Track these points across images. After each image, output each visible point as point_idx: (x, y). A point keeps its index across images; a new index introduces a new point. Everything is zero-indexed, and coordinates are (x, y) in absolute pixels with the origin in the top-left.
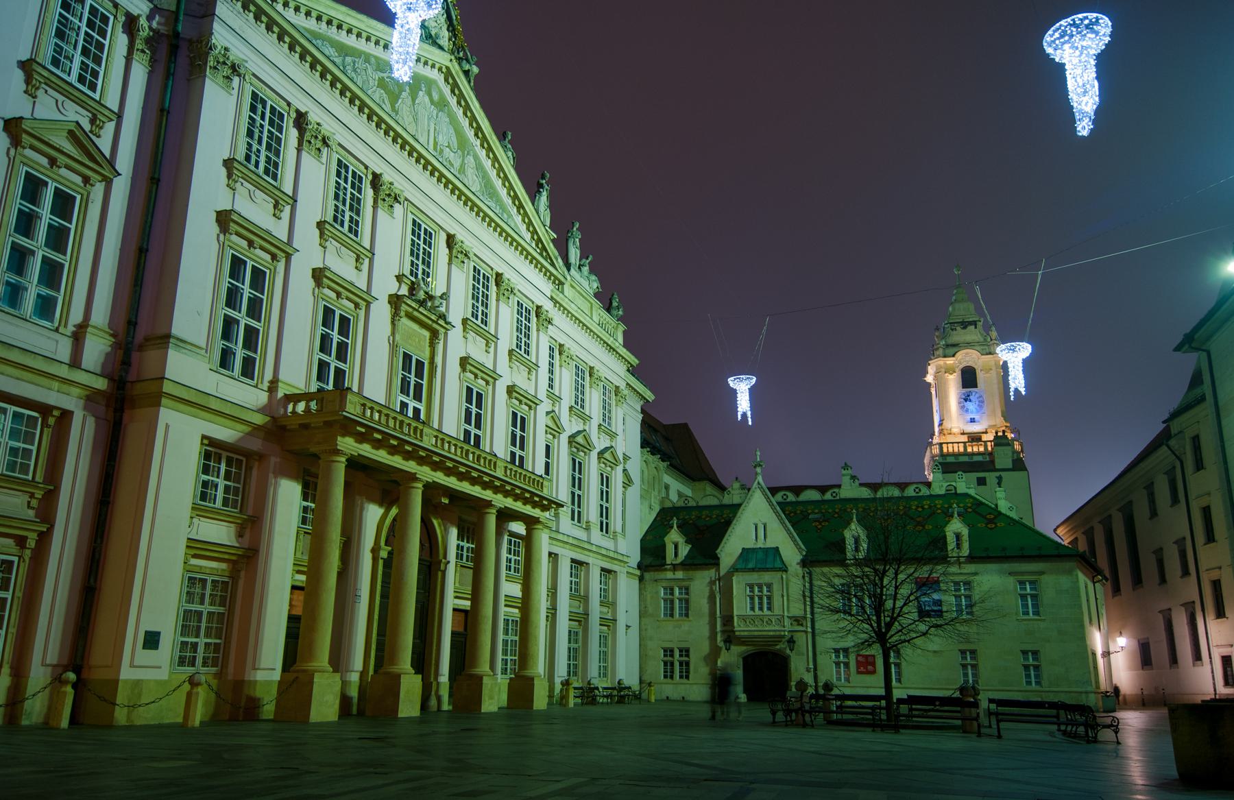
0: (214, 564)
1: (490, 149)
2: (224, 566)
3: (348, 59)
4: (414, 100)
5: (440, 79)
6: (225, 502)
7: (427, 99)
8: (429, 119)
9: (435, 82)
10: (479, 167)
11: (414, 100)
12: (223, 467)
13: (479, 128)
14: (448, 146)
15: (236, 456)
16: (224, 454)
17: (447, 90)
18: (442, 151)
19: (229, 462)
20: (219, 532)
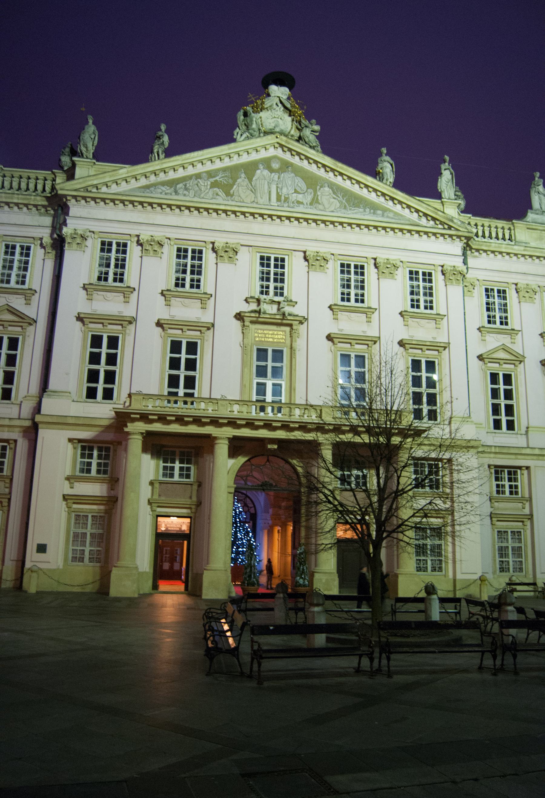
0: (95, 507)
1: (341, 174)
2: (102, 507)
3: (180, 185)
4: (250, 180)
5: (279, 152)
6: (98, 472)
7: (266, 172)
8: (269, 184)
9: (275, 157)
10: (336, 189)
11: (250, 180)
12: (95, 453)
13: (324, 166)
14: (296, 191)
15: (104, 445)
16: (95, 445)
17: (287, 156)
18: (286, 199)
19: (100, 449)
20: (95, 489)
